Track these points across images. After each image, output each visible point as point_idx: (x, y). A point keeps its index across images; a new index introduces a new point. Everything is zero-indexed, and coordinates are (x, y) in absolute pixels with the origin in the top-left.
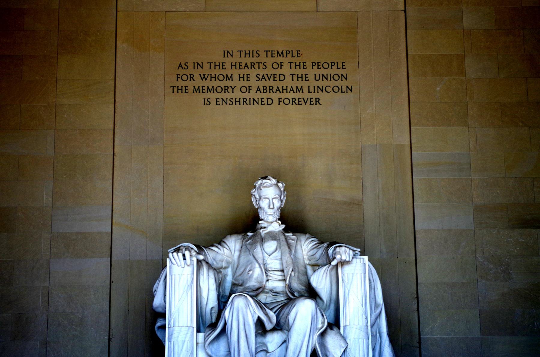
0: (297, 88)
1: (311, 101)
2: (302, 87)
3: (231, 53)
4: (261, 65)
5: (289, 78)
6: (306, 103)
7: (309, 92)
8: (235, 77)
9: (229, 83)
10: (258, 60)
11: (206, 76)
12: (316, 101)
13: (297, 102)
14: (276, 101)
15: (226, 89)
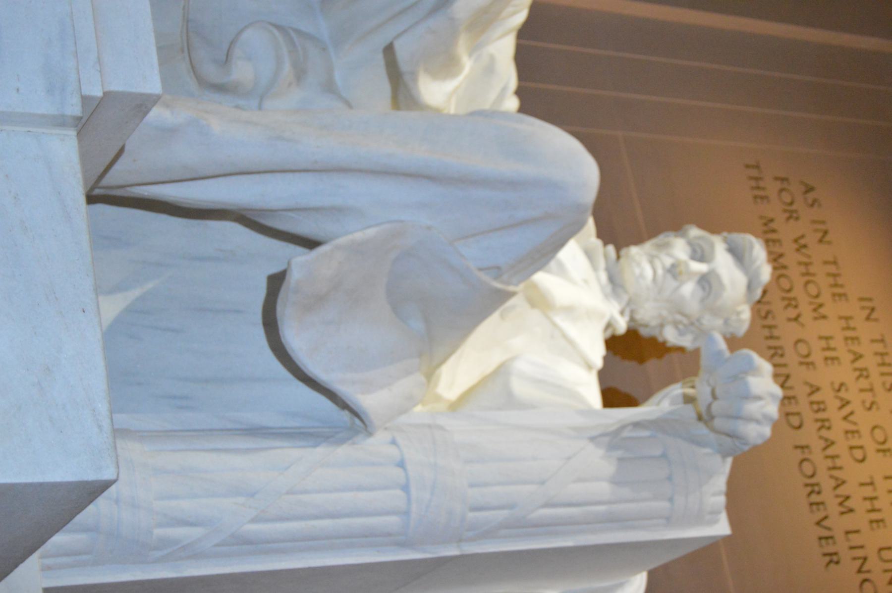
0: (848, 498)
1: (827, 538)
2: (851, 510)
3: (874, 316)
4: (868, 397)
5: (861, 473)
6: (818, 523)
7: (847, 533)
8: (824, 328)
9: (806, 310)
10: (878, 388)
11: (804, 250)
12: (831, 554)
13: (815, 498)
14: (802, 437)
15: (791, 303)
